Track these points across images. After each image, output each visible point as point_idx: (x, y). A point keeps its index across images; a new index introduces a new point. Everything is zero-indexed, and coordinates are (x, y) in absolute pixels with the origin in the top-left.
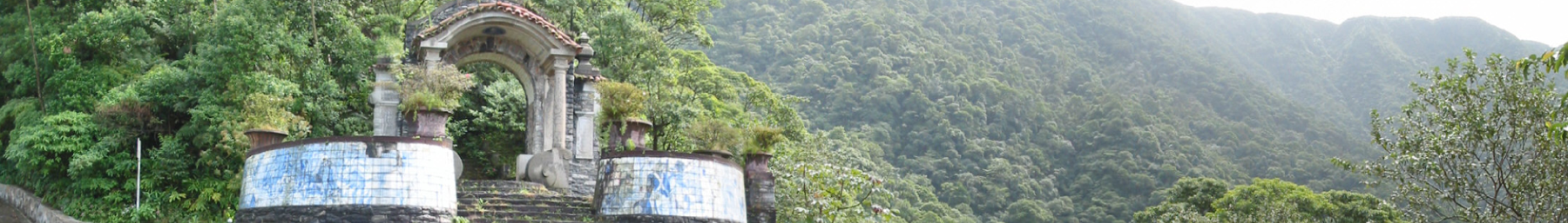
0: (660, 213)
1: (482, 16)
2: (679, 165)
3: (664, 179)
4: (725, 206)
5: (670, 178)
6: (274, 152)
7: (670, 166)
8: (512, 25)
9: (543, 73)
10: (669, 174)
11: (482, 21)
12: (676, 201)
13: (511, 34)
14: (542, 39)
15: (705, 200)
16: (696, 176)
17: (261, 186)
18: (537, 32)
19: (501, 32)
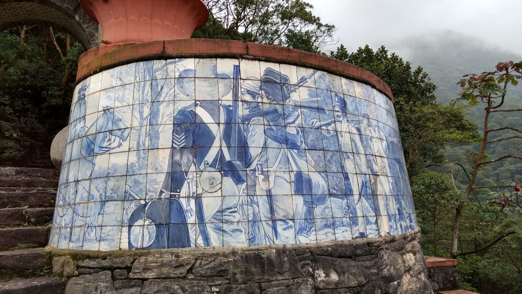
3: (229, 124)
5: (246, 119)
7: (245, 85)
10: (242, 111)
12: (270, 195)
15: (355, 184)
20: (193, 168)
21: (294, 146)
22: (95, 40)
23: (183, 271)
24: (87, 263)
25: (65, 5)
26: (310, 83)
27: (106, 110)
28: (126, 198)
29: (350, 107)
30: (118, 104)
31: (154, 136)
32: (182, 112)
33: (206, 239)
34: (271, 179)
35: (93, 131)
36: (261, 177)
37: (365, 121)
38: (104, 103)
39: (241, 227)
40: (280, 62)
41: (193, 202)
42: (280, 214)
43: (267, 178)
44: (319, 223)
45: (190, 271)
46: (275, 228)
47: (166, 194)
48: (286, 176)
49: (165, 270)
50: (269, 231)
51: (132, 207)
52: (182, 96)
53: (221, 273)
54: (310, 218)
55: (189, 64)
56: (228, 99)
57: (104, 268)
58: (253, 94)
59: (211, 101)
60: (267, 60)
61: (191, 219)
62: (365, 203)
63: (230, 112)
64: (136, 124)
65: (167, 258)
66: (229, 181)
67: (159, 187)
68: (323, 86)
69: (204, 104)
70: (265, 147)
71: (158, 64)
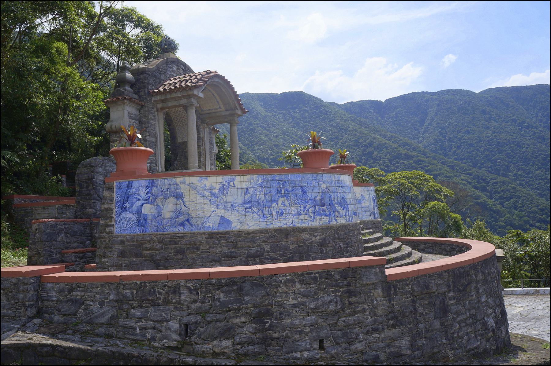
27: (362, 195)
28: (369, 211)
35: (359, 198)
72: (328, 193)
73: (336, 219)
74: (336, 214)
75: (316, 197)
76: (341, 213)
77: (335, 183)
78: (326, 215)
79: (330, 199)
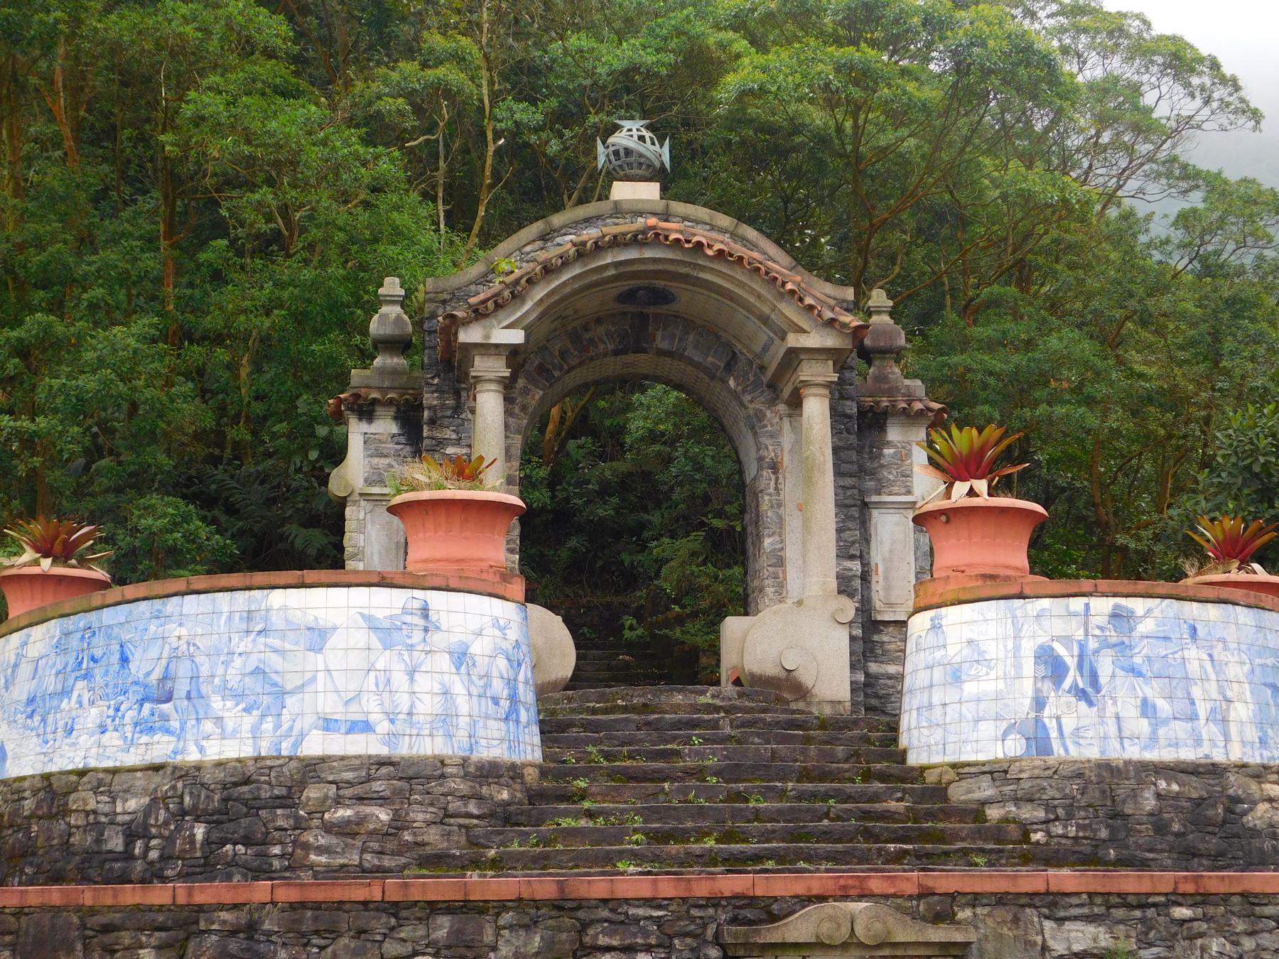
0: (1074, 753)
1: (609, 259)
2: (1117, 616)
4: (1260, 725)
5: (1096, 652)
6: (54, 627)
7: (1094, 621)
8: (685, 278)
9: (772, 402)
10: (1092, 644)
11: (612, 272)
12: (1118, 718)
13: (686, 300)
14: (766, 310)
15: (1202, 710)
16: (1172, 647)
17: (21, 718)
18: (752, 291)
19: (662, 297)
20: (1053, 694)
21: (1140, 674)
22: (765, 426)
23: (1050, 772)
24: (966, 770)
25: (710, 359)
26: (1157, 613)
27: (970, 642)
28: (998, 718)
29: (1201, 632)
30: (982, 637)
31: (1018, 667)
32: (1041, 647)
33: (1066, 750)
34: (1119, 703)
35: (958, 659)
36: (1110, 702)
37: (1220, 646)
38: (968, 634)
39: (1093, 741)
40: (1127, 596)
41: (1054, 721)
42: (1126, 733)
43: (1115, 703)
44: (1162, 742)
45: (1055, 773)
46: (1122, 744)
47: (1032, 715)
48: (1133, 701)
49: (1036, 772)
50: (1118, 746)
51: (1004, 725)
52: (1040, 632)
53: (1080, 775)
54: (1154, 738)
55: (1045, 603)
56: (1080, 635)
57: (984, 773)
58: (1101, 628)
59: (1066, 637)
60: (1115, 595)
61: (1054, 734)
62: (1214, 729)
63: (1082, 646)
64: (1001, 655)
65: (1037, 763)
66: (1083, 705)
67: (1026, 709)
68: (1171, 615)
69: (1059, 639)
70: (1113, 676)
71: (1017, 603)
72: (191, 656)
73: (204, 743)
74: (208, 726)
75: (148, 674)
76: (230, 725)
77: (230, 618)
78: (168, 731)
79: (194, 678)
